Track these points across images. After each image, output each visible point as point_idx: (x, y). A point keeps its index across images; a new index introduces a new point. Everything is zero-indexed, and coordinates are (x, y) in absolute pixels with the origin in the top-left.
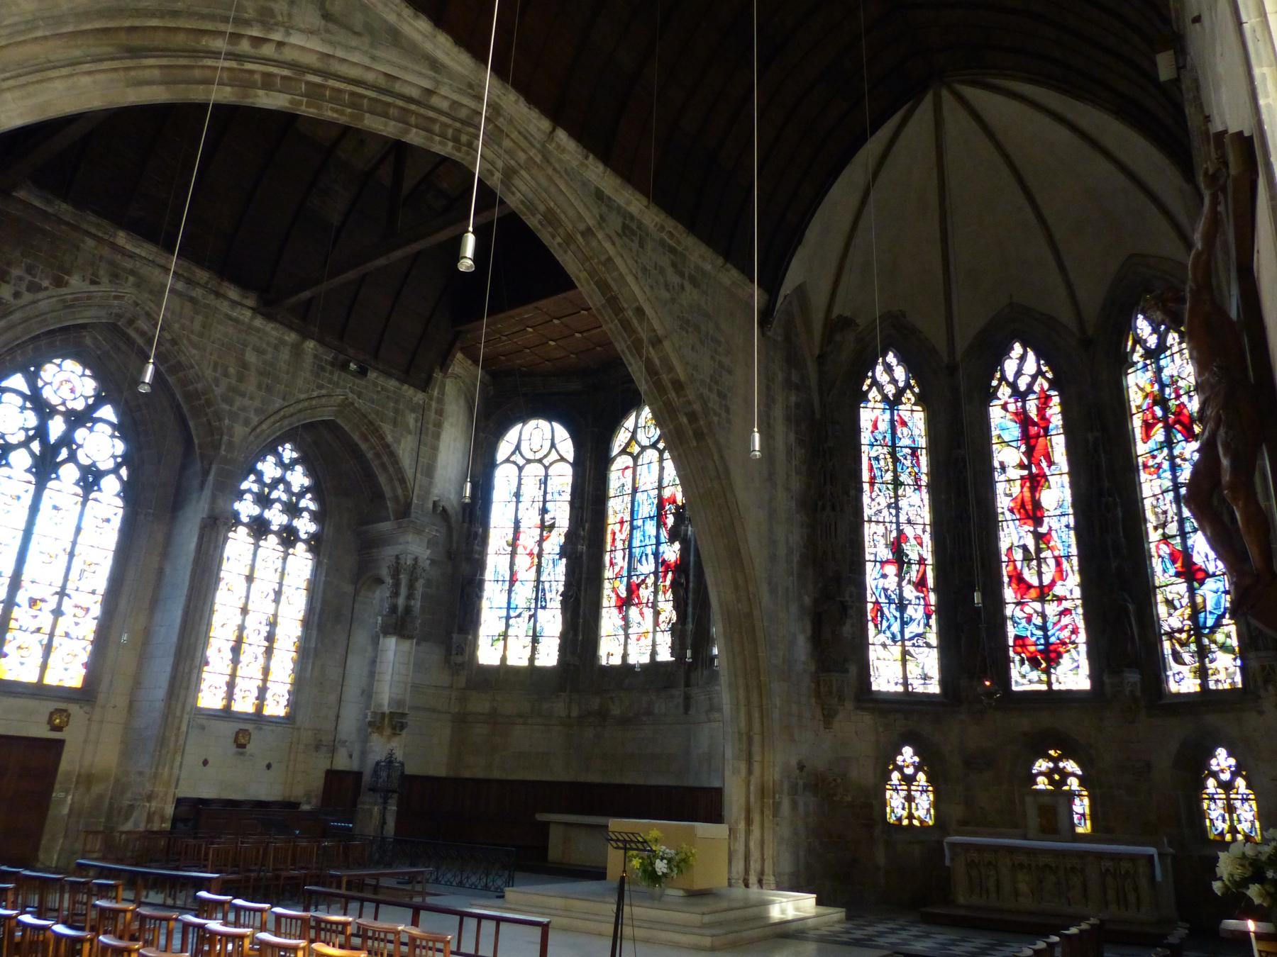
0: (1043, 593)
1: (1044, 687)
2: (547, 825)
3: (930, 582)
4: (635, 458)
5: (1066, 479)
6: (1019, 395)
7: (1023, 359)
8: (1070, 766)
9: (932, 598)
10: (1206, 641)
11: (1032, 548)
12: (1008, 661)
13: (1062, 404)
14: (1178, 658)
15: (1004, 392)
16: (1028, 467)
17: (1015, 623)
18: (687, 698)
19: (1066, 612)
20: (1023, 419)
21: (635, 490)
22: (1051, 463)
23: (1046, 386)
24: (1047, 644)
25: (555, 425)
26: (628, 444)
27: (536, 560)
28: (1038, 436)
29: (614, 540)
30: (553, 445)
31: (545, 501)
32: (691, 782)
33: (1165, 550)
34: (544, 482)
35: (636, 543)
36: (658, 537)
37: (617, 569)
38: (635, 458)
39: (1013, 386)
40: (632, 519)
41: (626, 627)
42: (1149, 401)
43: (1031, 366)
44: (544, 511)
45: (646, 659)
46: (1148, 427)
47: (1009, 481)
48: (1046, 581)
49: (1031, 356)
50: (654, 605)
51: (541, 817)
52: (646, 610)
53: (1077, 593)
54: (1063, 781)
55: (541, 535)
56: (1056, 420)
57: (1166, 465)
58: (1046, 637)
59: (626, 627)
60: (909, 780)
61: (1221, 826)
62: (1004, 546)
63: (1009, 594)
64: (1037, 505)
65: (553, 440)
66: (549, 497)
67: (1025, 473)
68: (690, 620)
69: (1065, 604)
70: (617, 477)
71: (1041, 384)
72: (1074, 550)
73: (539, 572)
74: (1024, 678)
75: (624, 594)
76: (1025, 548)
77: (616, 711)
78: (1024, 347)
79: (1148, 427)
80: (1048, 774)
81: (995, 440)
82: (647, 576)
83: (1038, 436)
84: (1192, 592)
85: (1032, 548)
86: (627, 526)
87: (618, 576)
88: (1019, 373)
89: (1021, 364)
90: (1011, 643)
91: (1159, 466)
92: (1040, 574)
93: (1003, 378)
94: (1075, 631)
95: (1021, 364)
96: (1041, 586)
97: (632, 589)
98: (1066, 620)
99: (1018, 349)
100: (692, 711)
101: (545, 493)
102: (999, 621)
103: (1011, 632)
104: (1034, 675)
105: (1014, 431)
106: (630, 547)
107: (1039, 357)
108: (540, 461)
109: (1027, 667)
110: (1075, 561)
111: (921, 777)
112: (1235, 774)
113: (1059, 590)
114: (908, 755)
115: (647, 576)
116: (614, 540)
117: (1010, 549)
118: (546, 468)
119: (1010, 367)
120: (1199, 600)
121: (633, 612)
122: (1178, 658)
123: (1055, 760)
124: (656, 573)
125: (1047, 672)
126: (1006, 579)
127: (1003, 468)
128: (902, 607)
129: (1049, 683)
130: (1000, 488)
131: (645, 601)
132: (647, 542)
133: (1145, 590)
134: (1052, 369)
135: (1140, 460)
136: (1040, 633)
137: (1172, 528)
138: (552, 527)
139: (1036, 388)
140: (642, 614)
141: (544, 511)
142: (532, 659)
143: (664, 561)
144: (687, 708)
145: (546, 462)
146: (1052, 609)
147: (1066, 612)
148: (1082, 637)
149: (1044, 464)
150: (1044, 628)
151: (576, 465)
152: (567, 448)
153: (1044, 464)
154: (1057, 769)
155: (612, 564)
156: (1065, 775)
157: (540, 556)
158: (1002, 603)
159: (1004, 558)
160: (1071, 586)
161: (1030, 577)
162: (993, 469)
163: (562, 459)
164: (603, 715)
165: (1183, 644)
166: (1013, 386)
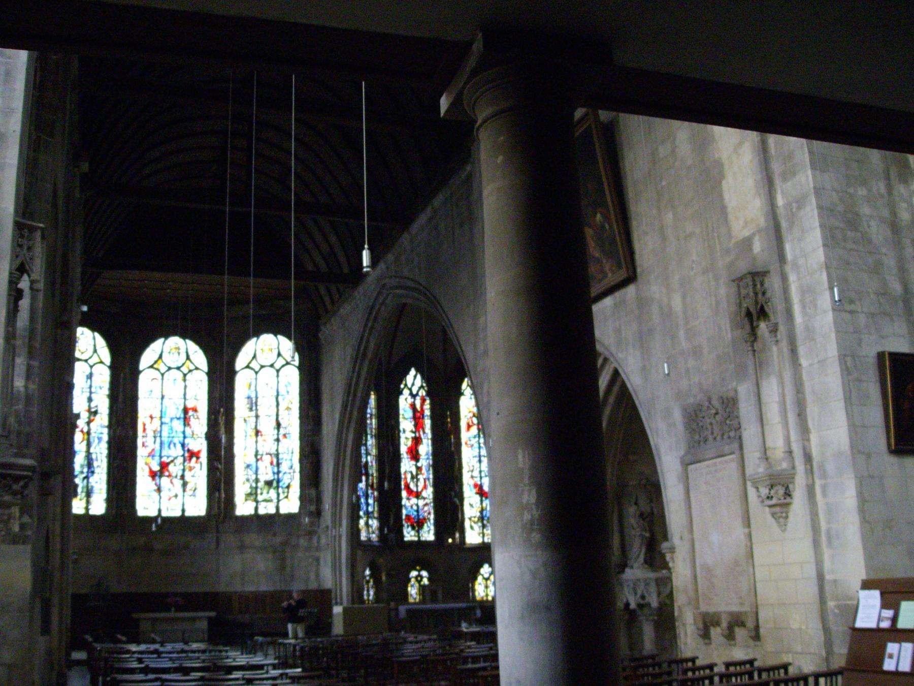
0: (418, 495)
1: (416, 539)
2: (138, 620)
3: (375, 486)
4: (163, 375)
5: (430, 442)
6: (414, 396)
7: (415, 377)
8: (424, 573)
9: (376, 493)
10: (485, 522)
11: (414, 473)
12: (402, 526)
13: (432, 404)
14: (472, 527)
15: (406, 392)
16: (414, 433)
17: (406, 508)
18: (218, 538)
19: (426, 505)
20: (413, 406)
21: (163, 397)
22: (424, 433)
23: (424, 394)
24: (419, 519)
25: (96, 334)
26: (156, 362)
27: (86, 437)
28: (419, 418)
29: (144, 430)
30: (95, 351)
31: (91, 393)
32: (222, 588)
33: (472, 482)
34: (90, 376)
35: (165, 434)
36: (184, 432)
37: (149, 450)
38: (163, 375)
39: (410, 390)
40: (161, 417)
41: (159, 490)
42: (471, 415)
43: (419, 381)
44: (90, 400)
45: (178, 514)
46: (469, 427)
47: (407, 438)
48: (420, 490)
49: (419, 377)
50: (183, 477)
51: (135, 616)
52: (175, 480)
53: (431, 496)
54: (421, 580)
55: (89, 418)
56: (427, 412)
57: (476, 445)
58: (418, 515)
59: (159, 490)
60: (368, 582)
61: (483, 594)
62: (403, 470)
63: (404, 494)
64: (417, 452)
65: (95, 346)
66: (93, 390)
67: (413, 435)
68: (222, 491)
69: (427, 501)
70: (147, 383)
71: (423, 393)
72: (431, 476)
73: (89, 445)
74: (409, 535)
75: (156, 468)
76: (411, 473)
77: (158, 546)
78: (417, 370)
79: (469, 427)
80: (416, 578)
81: (401, 416)
82: (176, 458)
83: (419, 418)
84: (482, 501)
85: (414, 473)
86: (157, 422)
87: (151, 455)
88: (413, 384)
89: (414, 380)
90: (404, 517)
91: (472, 446)
92: (417, 486)
93: (406, 385)
94: (429, 513)
95: (414, 380)
96: (417, 492)
97: (164, 466)
98: (426, 508)
99: (413, 372)
100: (222, 546)
101: (91, 387)
102: (400, 507)
103: (404, 512)
104: (413, 533)
105: (409, 414)
106: (161, 436)
107: (423, 377)
108: (86, 361)
109: (410, 529)
110: (431, 481)
111: (371, 583)
112: (490, 575)
113: (424, 494)
114: (368, 572)
115: (176, 458)
116: (144, 430)
117: (405, 472)
118: (91, 367)
119: (410, 378)
120: (484, 505)
121: (165, 481)
122: (472, 527)
123: (419, 571)
124: (183, 456)
125: (418, 532)
126: (403, 487)
127: (404, 431)
128: (367, 497)
129: (419, 537)
130: (402, 440)
131: (174, 475)
132: (174, 434)
133: (461, 499)
134: (427, 386)
135: (463, 440)
136: (415, 513)
137: (476, 473)
138: (96, 413)
139: (420, 394)
140: (171, 482)
141: (90, 400)
142: (87, 509)
143: (189, 450)
144: (218, 544)
145: (91, 362)
146: (421, 503)
147: (426, 505)
148: (432, 517)
149: (421, 433)
150: (417, 511)
151: (112, 367)
152: (105, 355)
153: (421, 433)
154: (419, 575)
155: (143, 445)
156: (422, 577)
157: (89, 433)
158: (401, 499)
159: (403, 476)
160: (429, 493)
161: (412, 486)
162: (399, 431)
163: (101, 362)
164: (148, 549)
165: (475, 523)
166: (410, 390)
